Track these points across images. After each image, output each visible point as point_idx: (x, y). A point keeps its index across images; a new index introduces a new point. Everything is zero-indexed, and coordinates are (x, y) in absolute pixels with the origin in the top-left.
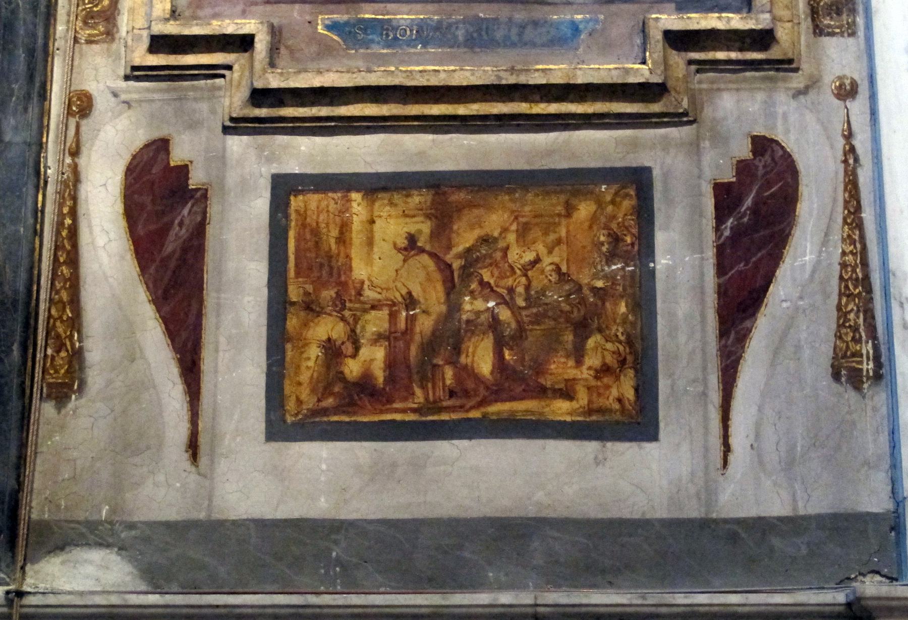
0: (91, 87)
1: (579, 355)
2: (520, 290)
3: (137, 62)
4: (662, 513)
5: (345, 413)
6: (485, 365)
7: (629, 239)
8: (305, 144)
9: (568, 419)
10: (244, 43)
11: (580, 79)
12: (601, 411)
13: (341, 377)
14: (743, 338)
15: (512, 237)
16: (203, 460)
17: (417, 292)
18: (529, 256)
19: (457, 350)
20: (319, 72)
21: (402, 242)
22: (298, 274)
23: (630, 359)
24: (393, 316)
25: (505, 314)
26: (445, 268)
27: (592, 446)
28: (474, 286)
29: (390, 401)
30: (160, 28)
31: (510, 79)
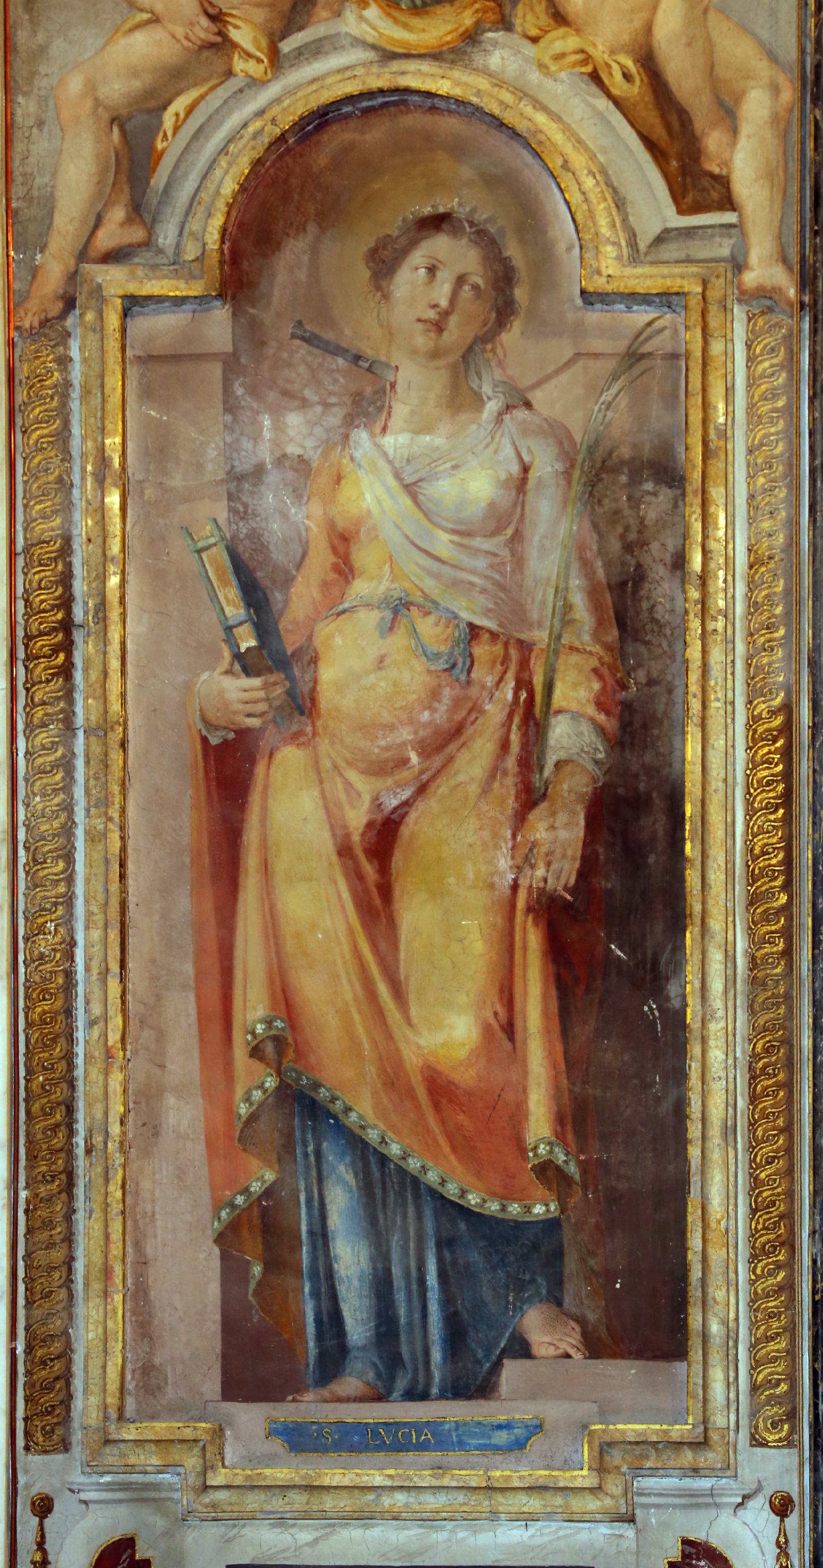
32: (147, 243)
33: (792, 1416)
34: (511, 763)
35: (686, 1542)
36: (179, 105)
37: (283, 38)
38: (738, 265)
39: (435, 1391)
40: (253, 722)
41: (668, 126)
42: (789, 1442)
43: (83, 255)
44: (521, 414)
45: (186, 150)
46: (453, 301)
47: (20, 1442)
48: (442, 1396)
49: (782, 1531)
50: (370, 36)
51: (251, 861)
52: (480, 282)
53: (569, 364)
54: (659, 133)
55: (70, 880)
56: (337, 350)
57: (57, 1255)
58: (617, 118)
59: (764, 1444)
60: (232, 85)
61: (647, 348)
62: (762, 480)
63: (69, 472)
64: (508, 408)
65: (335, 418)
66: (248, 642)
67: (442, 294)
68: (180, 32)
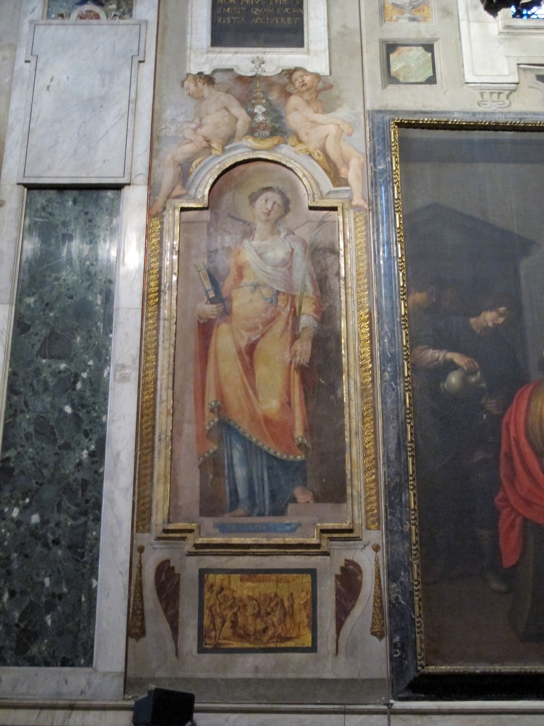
32: (187, 194)
33: (379, 520)
34: (289, 328)
35: (346, 560)
36: (197, 161)
37: (226, 145)
38: (351, 200)
39: (267, 513)
40: (213, 317)
41: (330, 167)
42: (378, 528)
43: (168, 197)
44: (292, 236)
45: (199, 171)
46: (272, 208)
47: (135, 530)
48: (270, 515)
49: (377, 557)
50: (249, 145)
51: (212, 355)
52: (280, 203)
53: (305, 224)
54: (328, 168)
55: (157, 360)
56: (238, 220)
57: (148, 471)
58: (316, 164)
59: (371, 529)
60: (211, 157)
61: (327, 220)
62: (360, 253)
64: (288, 234)
65: (239, 237)
66: (212, 295)
67: (269, 206)
68: (198, 144)
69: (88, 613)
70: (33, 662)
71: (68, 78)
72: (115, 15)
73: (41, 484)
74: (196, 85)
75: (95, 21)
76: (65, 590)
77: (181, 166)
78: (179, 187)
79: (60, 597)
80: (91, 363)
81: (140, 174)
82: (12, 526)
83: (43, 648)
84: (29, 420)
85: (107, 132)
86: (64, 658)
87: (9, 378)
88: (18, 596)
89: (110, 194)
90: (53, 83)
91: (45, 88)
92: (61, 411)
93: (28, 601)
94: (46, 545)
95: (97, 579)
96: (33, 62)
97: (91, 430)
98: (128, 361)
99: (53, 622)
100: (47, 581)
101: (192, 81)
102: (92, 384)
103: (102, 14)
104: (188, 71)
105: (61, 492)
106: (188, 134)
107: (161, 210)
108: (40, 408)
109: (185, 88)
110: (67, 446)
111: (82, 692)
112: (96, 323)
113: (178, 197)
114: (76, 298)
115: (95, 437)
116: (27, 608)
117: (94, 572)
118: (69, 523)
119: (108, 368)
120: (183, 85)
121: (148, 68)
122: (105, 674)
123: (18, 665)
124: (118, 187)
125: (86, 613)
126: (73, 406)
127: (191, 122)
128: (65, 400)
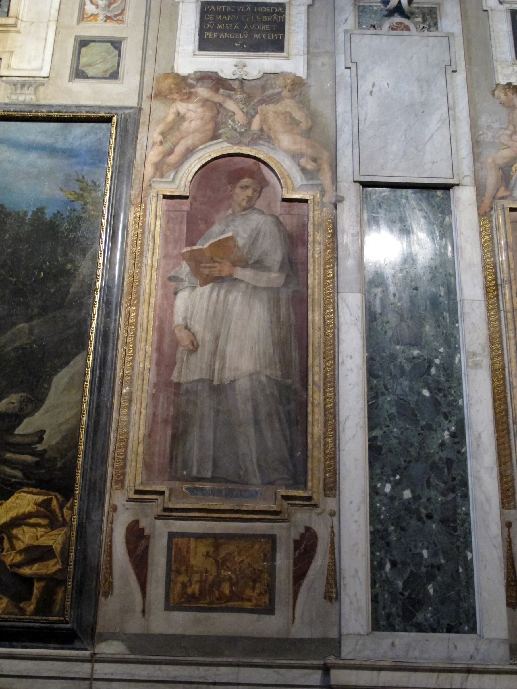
0: (116, 503)
1: (253, 588)
2: (238, 569)
3: (131, 497)
4: (276, 636)
5: (187, 603)
6: (227, 592)
7: (269, 556)
8: (178, 523)
9: (250, 608)
10: (162, 493)
11: (257, 509)
12: (259, 606)
13: (186, 593)
14: (300, 585)
15: (236, 554)
16: (146, 616)
17: (209, 569)
18: (241, 559)
19: (219, 586)
20: (183, 503)
21: (205, 554)
22: (175, 562)
23: (268, 591)
24: (202, 575)
25: (233, 576)
26: (217, 561)
27: (256, 616)
28: (225, 567)
29: (200, 600)
30: (138, 488)
31: (237, 508)
32: (510, 195)
43: (494, 198)
55: (502, 350)
57: (507, 452)
63: (494, 247)
69: (466, 583)
70: (420, 628)
71: (388, 84)
72: (423, 28)
73: (410, 462)
74: (506, 95)
75: (406, 33)
76: (443, 561)
77: (502, 170)
78: (502, 189)
79: (439, 567)
80: (442, 350)
81: (466, 176)
82: (386, 500)
83: (429, 615)
84: (389, 401)
85: (432, 136)
86: (448, 625)
87: (367, 362)
88: (399, 566)
89: (439, 193)
90: (375, 89)
91: (369, 93)
92: (420, 394)
93: (409, 571)
94: (420, 519)
95: (472, 552)
96: (354, 69)
97: (450, 412)
98: (478, 350)
99: (435, 591)
100: (425, 553)
101: (502, 91)
102: (445, 370)
103: (412, 26)
104: (498, 82)
105: (429, 469)
106: (504, 139)
107: (488, 210)
108: (399, 392)
109: (496, 97)
110: (429, 427)
111: (472, 657)
112: (442, 313)
113: (502, 198)
114: (421, 290)
115: (454, 419)
116: (409, 577)
117: (468, 545)
118: (439, 499)
119: (458, 355)
120: (493, 95)
121: (460, 78)
122: (490, 641)
123: (406, 631)
124: (447, 188)
125: (464, 583)
126: (430, 390)
127: (506, 129)
128: (422, 384)
